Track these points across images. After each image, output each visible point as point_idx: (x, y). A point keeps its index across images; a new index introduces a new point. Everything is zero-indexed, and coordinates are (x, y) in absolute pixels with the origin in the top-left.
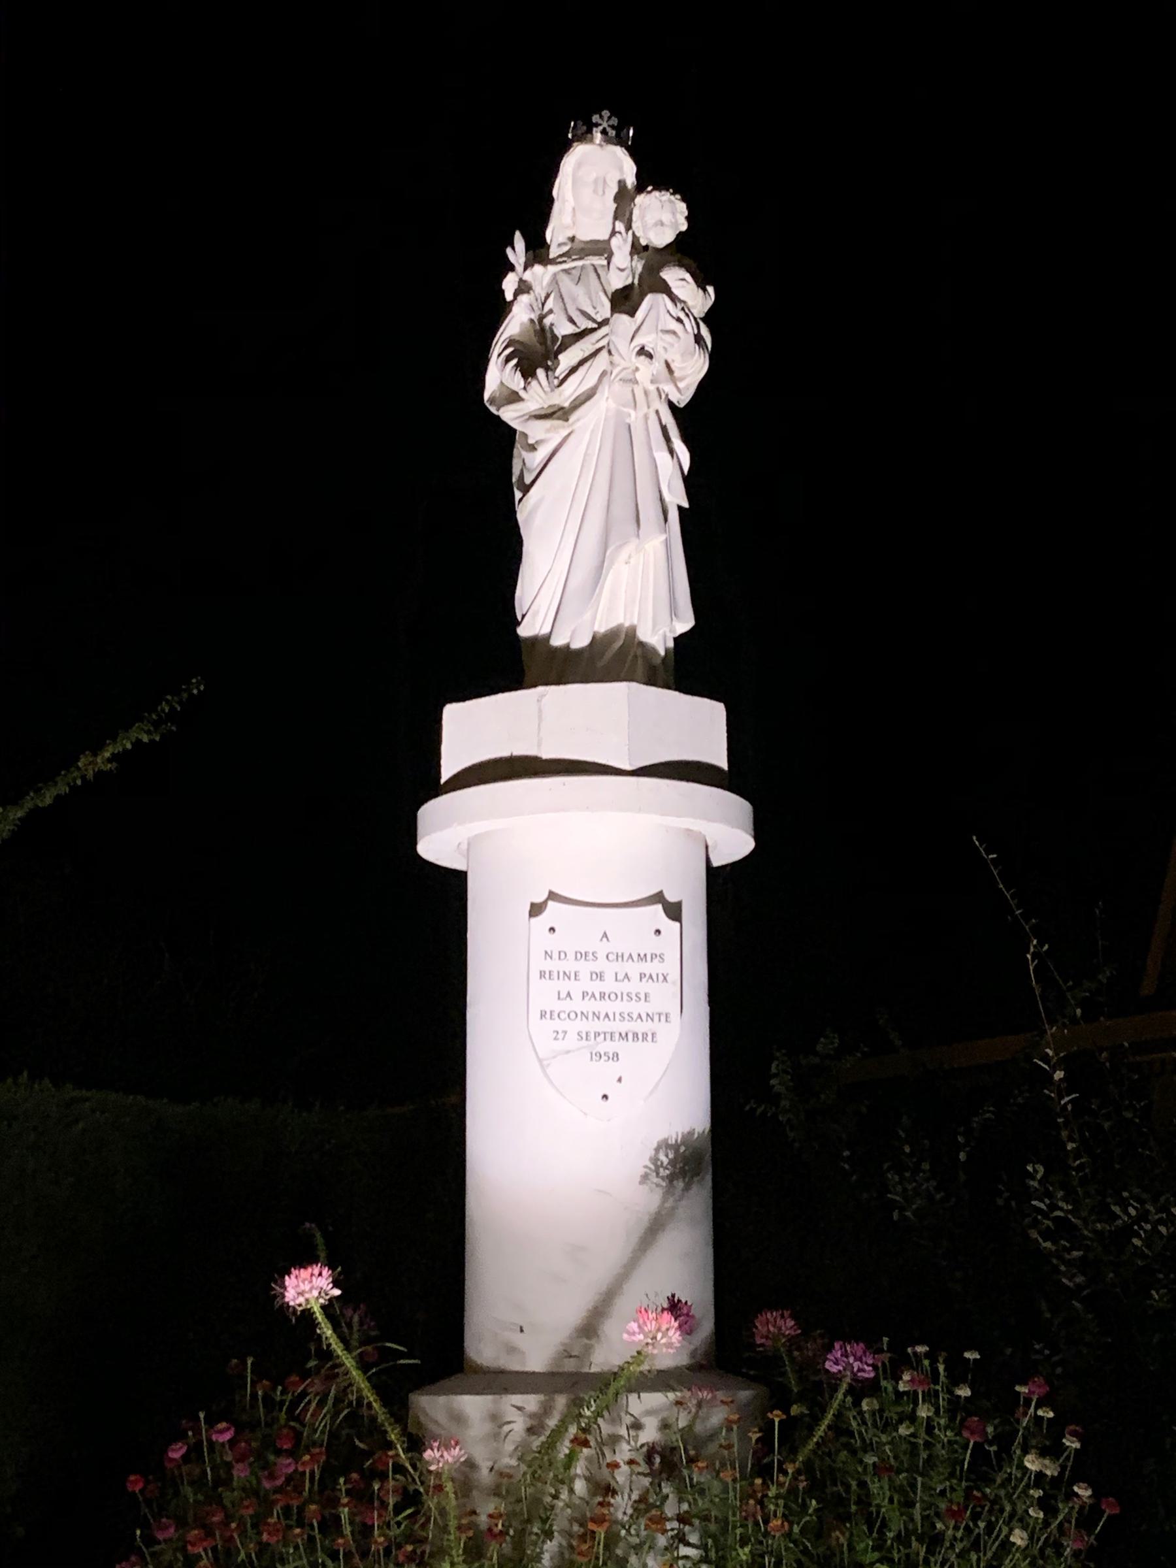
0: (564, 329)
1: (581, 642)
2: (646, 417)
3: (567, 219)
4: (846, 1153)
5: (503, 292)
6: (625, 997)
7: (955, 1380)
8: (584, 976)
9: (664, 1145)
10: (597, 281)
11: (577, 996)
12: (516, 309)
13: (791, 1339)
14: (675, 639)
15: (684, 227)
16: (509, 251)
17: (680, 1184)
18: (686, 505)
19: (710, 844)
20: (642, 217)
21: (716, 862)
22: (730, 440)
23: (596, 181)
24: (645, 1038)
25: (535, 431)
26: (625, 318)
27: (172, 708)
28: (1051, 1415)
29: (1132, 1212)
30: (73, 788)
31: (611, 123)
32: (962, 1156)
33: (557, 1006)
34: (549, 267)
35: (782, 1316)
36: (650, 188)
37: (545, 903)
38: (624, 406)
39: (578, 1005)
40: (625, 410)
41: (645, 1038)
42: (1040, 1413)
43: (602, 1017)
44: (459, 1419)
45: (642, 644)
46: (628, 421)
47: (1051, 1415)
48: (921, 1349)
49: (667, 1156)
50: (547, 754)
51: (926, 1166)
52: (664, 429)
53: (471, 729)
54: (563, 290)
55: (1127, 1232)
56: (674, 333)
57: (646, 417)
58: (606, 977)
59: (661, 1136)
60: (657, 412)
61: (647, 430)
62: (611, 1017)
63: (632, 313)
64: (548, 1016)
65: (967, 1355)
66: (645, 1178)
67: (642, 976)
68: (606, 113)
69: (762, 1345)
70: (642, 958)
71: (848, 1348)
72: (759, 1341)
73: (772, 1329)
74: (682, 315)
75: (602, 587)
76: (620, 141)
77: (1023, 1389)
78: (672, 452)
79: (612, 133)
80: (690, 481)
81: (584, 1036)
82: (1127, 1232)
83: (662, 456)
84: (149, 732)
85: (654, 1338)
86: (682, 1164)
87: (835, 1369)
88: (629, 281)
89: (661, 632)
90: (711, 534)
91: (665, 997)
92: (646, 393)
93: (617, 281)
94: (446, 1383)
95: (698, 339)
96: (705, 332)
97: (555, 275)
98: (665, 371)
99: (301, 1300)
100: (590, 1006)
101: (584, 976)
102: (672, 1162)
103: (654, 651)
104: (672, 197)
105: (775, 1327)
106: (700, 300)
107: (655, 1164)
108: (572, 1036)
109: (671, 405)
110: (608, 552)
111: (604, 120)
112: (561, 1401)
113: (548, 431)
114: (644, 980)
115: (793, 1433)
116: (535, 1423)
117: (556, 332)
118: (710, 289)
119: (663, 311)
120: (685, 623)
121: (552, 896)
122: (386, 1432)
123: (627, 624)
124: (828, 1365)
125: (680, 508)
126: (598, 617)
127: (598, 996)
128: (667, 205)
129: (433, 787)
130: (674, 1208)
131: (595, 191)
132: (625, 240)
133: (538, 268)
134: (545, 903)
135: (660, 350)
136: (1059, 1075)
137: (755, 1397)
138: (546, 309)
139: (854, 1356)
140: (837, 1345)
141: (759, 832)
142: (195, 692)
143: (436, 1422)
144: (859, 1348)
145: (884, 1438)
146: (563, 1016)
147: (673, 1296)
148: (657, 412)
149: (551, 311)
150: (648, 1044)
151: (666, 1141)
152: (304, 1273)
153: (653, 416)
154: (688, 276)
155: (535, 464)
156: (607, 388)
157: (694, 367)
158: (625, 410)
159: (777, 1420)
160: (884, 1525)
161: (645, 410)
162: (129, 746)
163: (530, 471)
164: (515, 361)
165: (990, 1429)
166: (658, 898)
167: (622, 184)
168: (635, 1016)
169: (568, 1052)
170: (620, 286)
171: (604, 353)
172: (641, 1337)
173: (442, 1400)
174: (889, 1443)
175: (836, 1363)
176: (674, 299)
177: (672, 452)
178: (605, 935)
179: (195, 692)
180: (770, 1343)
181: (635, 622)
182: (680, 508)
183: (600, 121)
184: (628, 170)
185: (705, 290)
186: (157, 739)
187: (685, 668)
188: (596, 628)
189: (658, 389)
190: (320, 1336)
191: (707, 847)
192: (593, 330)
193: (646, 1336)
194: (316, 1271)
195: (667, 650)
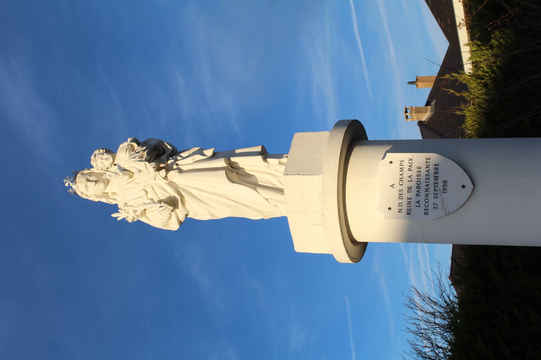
11: (418, 199)
16: (118, 219)
24: (437, 169)
33: (423, 207)
39: (422, 198)
43: (428, 188)
64: (427, 211)
81: (435, 196)
100: (423, 193)
127: (419, 189)
146: (427, 205)
150: (440, 168)
168: (427, 173)
169: (443, 203)
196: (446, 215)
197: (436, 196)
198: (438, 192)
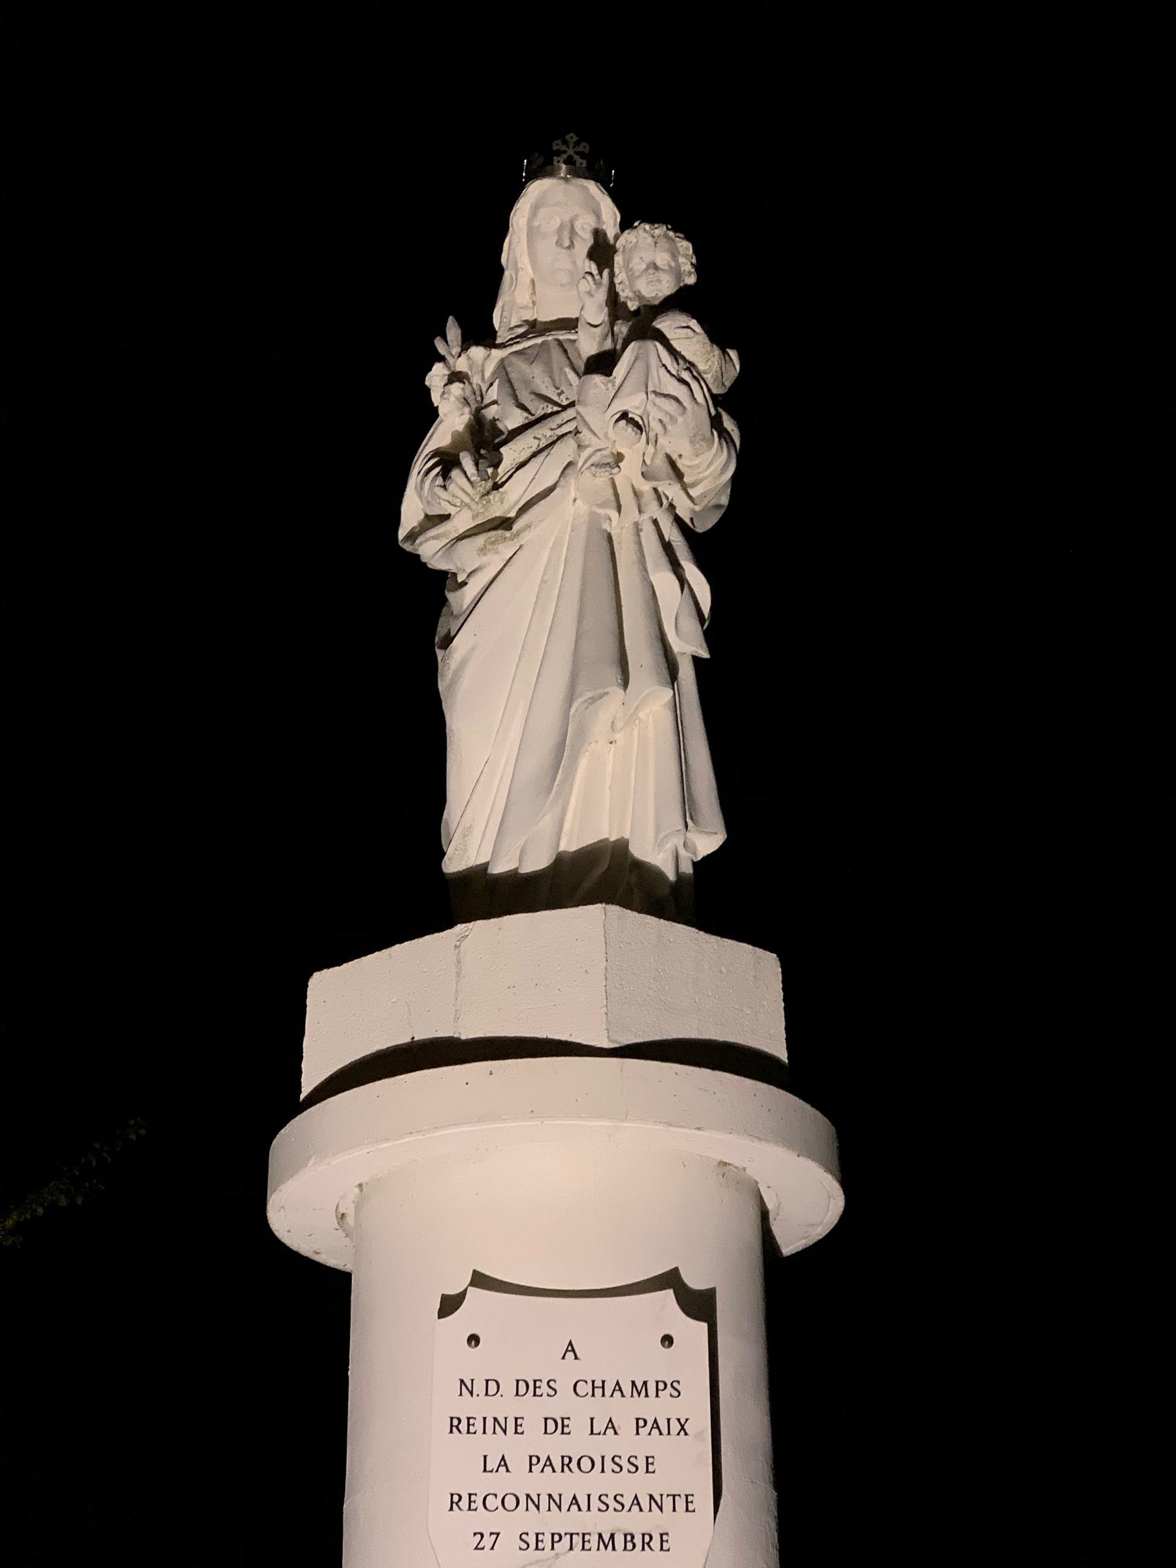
0: (513, 419)
1: (537, 861)
2: (637, 529)
5: (427, 391)
6: (609, 1465)
10: (563, 359)
11: (518, 1463)
15: (691, 280)
18: (705, 655)
19: (770, 1206)
20: (627, 262)
21: (789, 1246)
22: (791, 639)
23: (560, 230)
24: (646, 1545)
25: (464, 560)
26: (597, 379)
31: (580, 149)
33: (482, 1484)
34: (495, 352)
36: (636, 224)
37: (464, 1293)
38: (600, 506)
39: (521, 1481)
40: (602, 511)
41: (646, 1545)
43: (565, 1507)
45: (639, 866)
46: (606, 526)
50: (468, 1032)
52: (667, 547)
53: (348, 1007)
54: (513, 375)
56: (677, 400)
57: (637, 529)
61: (640, 544)
62: (584, 1506)
63: (609, 374)
64: (464, 1504)
67: (640, 1423)
70: (640, 1389)
74: (686, 376)
76: (593, 173)
78: (683, 581)
79: (581, 163)
80: (716, 629)
83: (665, 581)
88: (608, 345)
89: (669, 846)
90: (749, 704)
91: (685, 1464)
92: (637, 494)
93: (588, 344)
96: (728, 423)
97: (502, 360)
98: (670, 471)
100: (543, 1483)
101: (532, 1425)
103: (658, 875)
104: (671, 234)
108: (509, 1541)
109: (678, 520)
110: (573, 710)
111: (571, 143)
113: (483, 551)
114: (644, 1431)
117: (500, 425)
118: (733, 354)
119: (654, 362)
120: (708, 841)
121: (480, 1280)
123: (612, 839)
125: (696, 660)
126: (567, 826)
127: (557, 1464)
128: (663, 243)
129: (287, 1102)
131: (559, 243)
132: (598, 284)
133: (477, 352)
134: (464, 1293)
135: (656, 427)
138: (486, 401)
142: (133, 1137)
149: (495, 402)
150: (653, 1556)
154: (694, 323)
155: (465, 607)
156: (573, 481)
157: (711, 471)
158: (602, 511)
162: (40, 1211)
163: (456, 617)
164: (438, 470)
166: (671, 1280)
167: (599, 235)
168: (627, 1502)
170: (593, 351)
177: (683, 581)
178: (571, 1347)
179: (133, 1137)
181: (627, 836)
182: (696, 660)
183: (564, 148)
184: (609, 215)
185: (724, 352)
186: (79, 1201)
188: (562, 848)
189: (655, 490)
191: (764, 1215)
192: (557, 413)
195: (678, 874)
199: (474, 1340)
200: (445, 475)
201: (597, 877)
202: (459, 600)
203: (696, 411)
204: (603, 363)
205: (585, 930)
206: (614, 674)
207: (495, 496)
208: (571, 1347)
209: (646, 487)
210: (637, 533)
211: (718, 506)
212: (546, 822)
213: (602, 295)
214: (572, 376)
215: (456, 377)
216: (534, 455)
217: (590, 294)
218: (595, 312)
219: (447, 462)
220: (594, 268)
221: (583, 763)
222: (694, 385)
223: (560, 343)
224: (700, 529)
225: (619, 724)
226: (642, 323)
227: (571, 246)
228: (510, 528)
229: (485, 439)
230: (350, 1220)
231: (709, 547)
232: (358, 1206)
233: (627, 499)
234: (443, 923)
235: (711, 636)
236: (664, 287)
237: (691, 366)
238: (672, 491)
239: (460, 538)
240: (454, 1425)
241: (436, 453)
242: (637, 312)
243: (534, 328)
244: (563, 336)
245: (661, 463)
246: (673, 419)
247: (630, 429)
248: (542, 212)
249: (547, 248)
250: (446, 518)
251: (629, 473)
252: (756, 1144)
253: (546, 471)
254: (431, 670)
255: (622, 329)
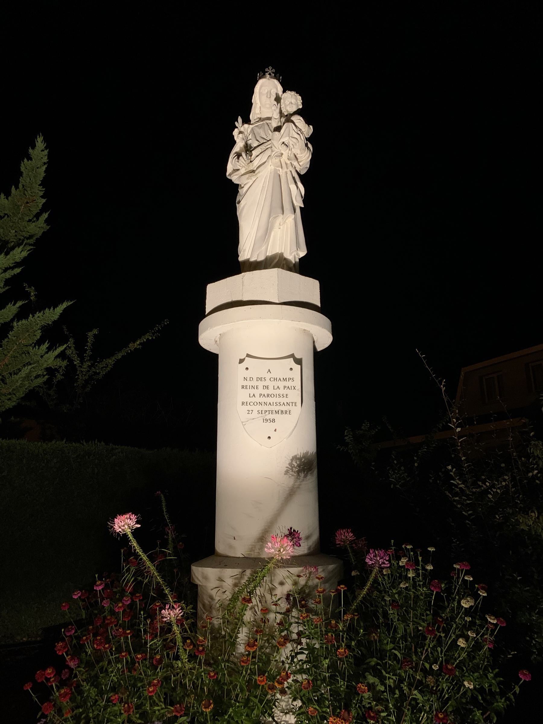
1: (261, 258)
2: (286, 173)
3: (258, 111)
4: (373, 464)
5: (233, 136)
6: (278, 396)
7: (425, 562)
8: (260, 387)
9: (295, 458)
11: (257, 395)
12: (237, 142)
13: (351, 542)
14: (299, 259)
15: (301, 107)
16: (236, 123)
17: (302, 475)
18: (303, 206)
19: (315, 340)
20: (284, 102)
21: (319, 349)
24: (286, 413)
26: (277, 133)
27: (158, 328)
28: (472, 579)
29: (488, 484)
30: (127, 353)
32: (416, 465)
35: (348, 532)
39: (258, 399)
42: (466, 578)
44: (206, 578)
46: (278, 172)
47: (472, 579)
48: (409, 547)
49: (296, 463)
50: (245, 299)
51: (402, 468)
52: (294, 178)
53: (216, 292)
54: (255, 132)
55: (486, 492)
57: (286, 173)
58: (269, 387)
59: (293, 455)
60: (291, 171)
61: (287, 177)
64: (245, 404)
65: (429, 549)
66: (287, 472)
67: (285, 387)
68: (270, 68)
69: (339, 544)
71: (377, 552)
72: (338, 542)
73: (343, 537)
74: (299, 132)
75: (269, 236)
76: (275, 77)
77: (456, 566)
78: (297, 187)
80: (306, 200)
81: (260, 412)
82: (486, 492)
83: (293, 187)
84: (151, 336)
85: (280, 551)
86: (302, 466)
87: (371, 562)
88: (279, 124)
90: (314, 217)
91: (295, 396)
92: (286, 164)
93: (274, 124)
94: (204, 561)
95: (306, 145)
96: (310, 145)
99: (120, 530)
101: (260, 387)
102: (299, 466)
103: (291, 262)
105: (344, 536)
106: (308, 130)
107: (291, 466)
108: (255, 412)
109: (296, 171)
111: (270, 70)
112: (248, 572)
113: (248, 179)
115: (351, 592)
116: (237, 581)
117: (252, 145)
118: (311, 127)
120: (303, 253)
121: (248, 356)
122: (163, 589)
124: (367, 560)
125: (300, 207)
127: (266, 396)
128: (294, 96)
129: (202, 315)
130: (300, 485)
131: (267, 97)
132: (277, 108)
133: (246, 126)
136: (459, 430)
137: (336, 568)
139: (380, 556)
140: (371, 552)
141: (334, 332)
143: (198, 579)
144: (382, 553)
145: (394, 591)
146: (251, 404)
147: (291, 528)
148: (291, 171)
151: (296, 456)
152: (122, 517)
153: (289, 173)
154: (301, 118)
159: (342, 590)
160: (395, 631)
161: (286, 170)
162: (145, 340)
165: (443, 586)
166: (292, 356)
167: (277, 94)
168: (282, 404)
170: (276, 126)
171: (270, 149)
172: (273, 550)
173: (200, 569)
174: (396, 593)
175: (371, 560)
176: (295, 126)
177: (297, 187)
178: (269, 370)
180: (343, 543)
182: (300, 207)
184: (280, 88)
185: (309, 125)
186: (154, 338)
187: (303, 267)
188: (267, 254)
190: (131, 546)
191: (314, 342)
193: (275, 551)
194: (128, 516)
196: (242, 422)
197: (260, 412)
198: (264, 414)
199: (247, 369)
200: (238, 158)
201: (276, 262)
202: (241, 191)
203: (302, 141)
204: (278, 129)
205: (273, 273)
206: (280, 211)
207: (251, 164)
208: (269, 370)
209: (288, 162)
210: (287, 175)
211: (307, 168)
212: (264, 248)
213: (278, 111)
214: (270, 132)
215: (240, 132)
216: (261, 153)
217: (275, 110)
218: (276, 115)
219: (239, 155)
220: (276, 103)
221: (273, 234)
222: (301, 135)
223: (267, 124)
224: (302, 174)
225: (281, 224)
226: (288, 118)
227: (270, 97)
228: (254, 172)
229: (248, 149)
230: (218, 342)
231: (304, 178)
232: (220, 339)
233: (284, 165)
234: (238, 272)
235: (304, 201)
236: (294, 109)
237: (300, 130)
238: (295, 163)
239: (242, 175)
240: (243, 387)
241: (236, 153)
242: (287, 116)
243: (260, 119)
244: (268, 122)
245: (292, 156)
246: (296, 144)
247: (285, 146)
248: (263, 88)
249: (264, 98)
250: (238, 170)
251: (284, 158)
252: (313, 325)
253: (263, 158)
254: (235, 209)
255: (283, 120)
